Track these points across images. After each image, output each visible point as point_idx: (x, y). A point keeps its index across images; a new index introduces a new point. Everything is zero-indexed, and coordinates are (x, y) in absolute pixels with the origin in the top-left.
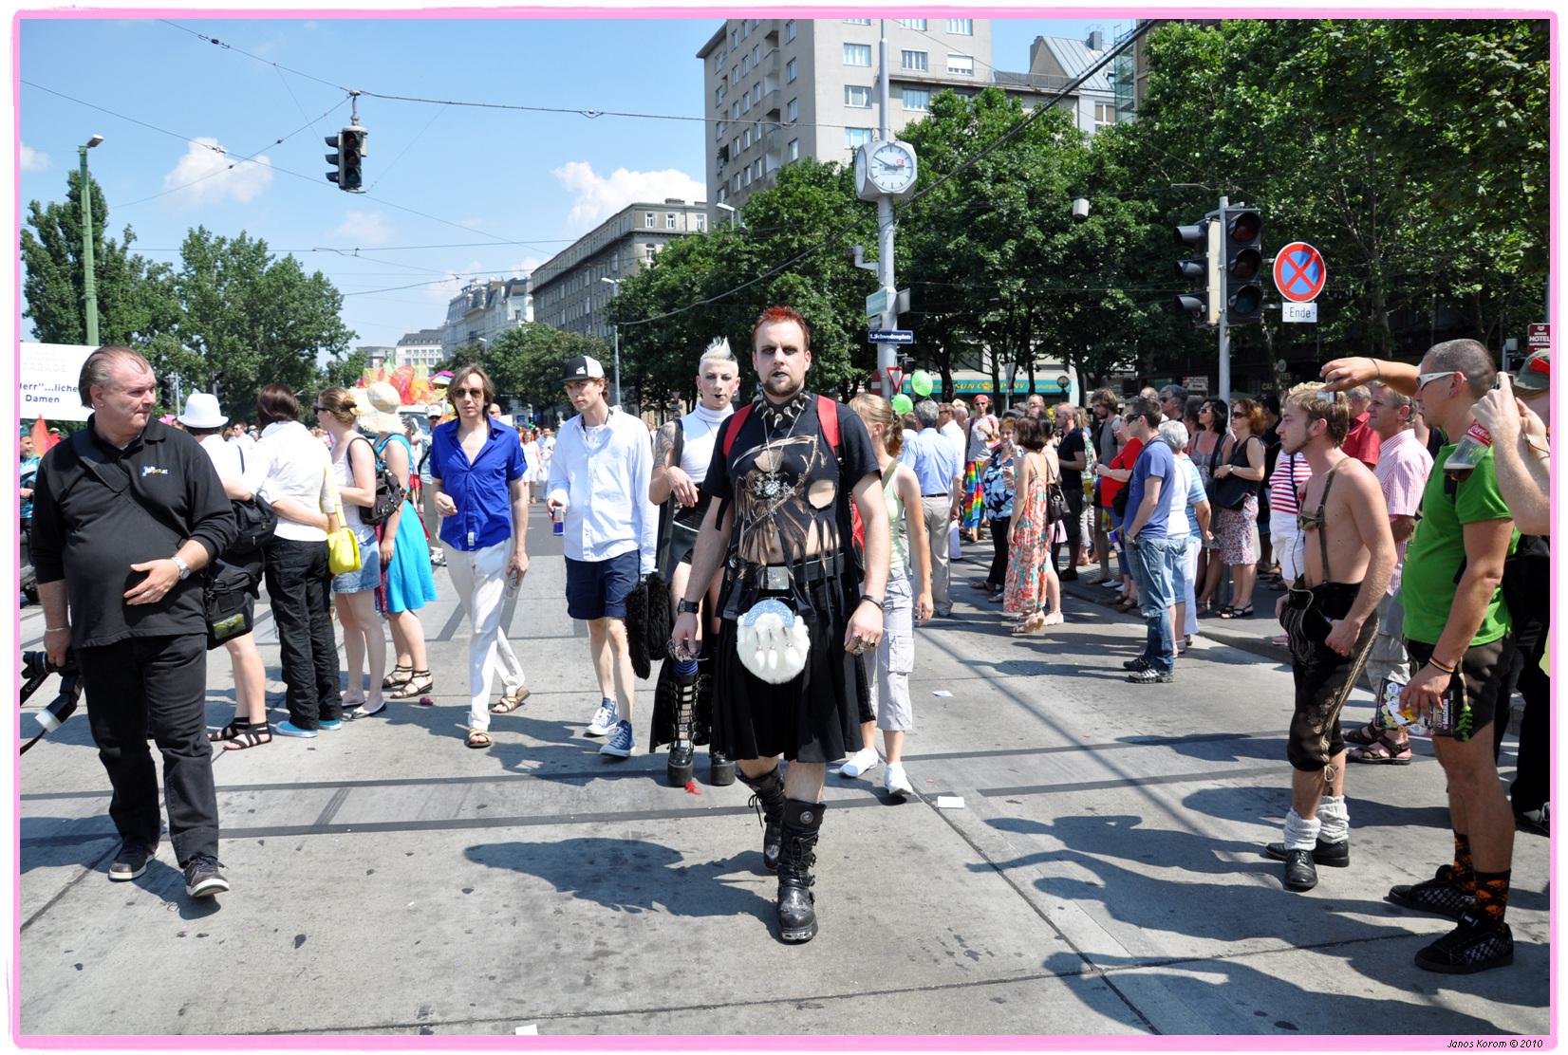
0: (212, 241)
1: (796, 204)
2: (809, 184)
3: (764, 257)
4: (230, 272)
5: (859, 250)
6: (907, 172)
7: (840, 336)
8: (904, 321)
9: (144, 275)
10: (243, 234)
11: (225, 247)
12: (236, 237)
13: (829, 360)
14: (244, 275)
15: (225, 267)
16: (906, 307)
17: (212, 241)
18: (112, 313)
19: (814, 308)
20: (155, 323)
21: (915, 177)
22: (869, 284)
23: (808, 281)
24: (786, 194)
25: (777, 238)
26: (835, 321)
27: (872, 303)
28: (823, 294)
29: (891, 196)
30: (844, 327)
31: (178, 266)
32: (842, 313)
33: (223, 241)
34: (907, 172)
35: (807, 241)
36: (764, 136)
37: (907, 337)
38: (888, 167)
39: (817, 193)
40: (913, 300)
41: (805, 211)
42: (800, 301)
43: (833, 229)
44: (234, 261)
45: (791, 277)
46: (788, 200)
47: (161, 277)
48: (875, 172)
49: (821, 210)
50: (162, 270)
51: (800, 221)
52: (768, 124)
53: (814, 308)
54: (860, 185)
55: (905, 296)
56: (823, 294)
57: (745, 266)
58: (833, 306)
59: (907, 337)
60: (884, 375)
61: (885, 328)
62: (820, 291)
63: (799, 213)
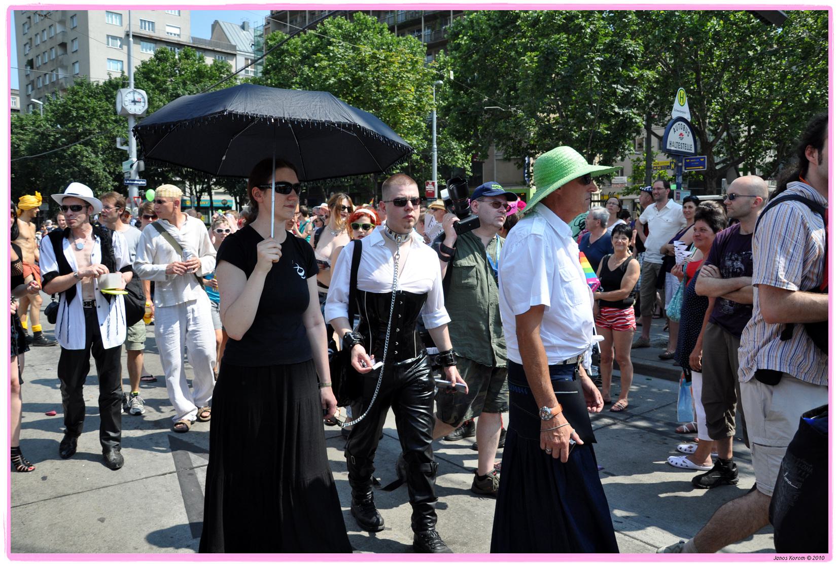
1: (82, 109)
2: (89, 96)
3: (63, 134)
5: (118, 139)
6: (142, 104)
7: (106, 177)
8: (141, 174)
13: (100, 190)
16: (142, 168)
19: (93, 163)
21: (146, 107)
22: (125, 156)
23: (89, 149)
24: (75, 102)
25: (70, 125)
26: (104, 170)
27: (125, 166)
28: (97, 156)
29: (134, 115)
30: (110, 173)
32: (108, 165)
34: (142, 104)
35: (87, 127)
36: (57, 57)
37: (143, 183)
38: (134, 102)
39: (93, 103)
40: (146, 165)
41: (87, 111)
42: (85, 159)
43: (102, 122)
45: (79, 147)
46: (76, 105)
48: (127, 103)
49: (95, 111)
51: (83, 117)
52: (60, 51)
53: (93, 163)
54: (119, 108)
55: (142, 163)
56: (97, 156)
57: (52, 138)
58: (103, 162)
59: (143, 183)
60: (133, 200)
61: (132, 178)
62: (96, 153)
63: (82, 112)
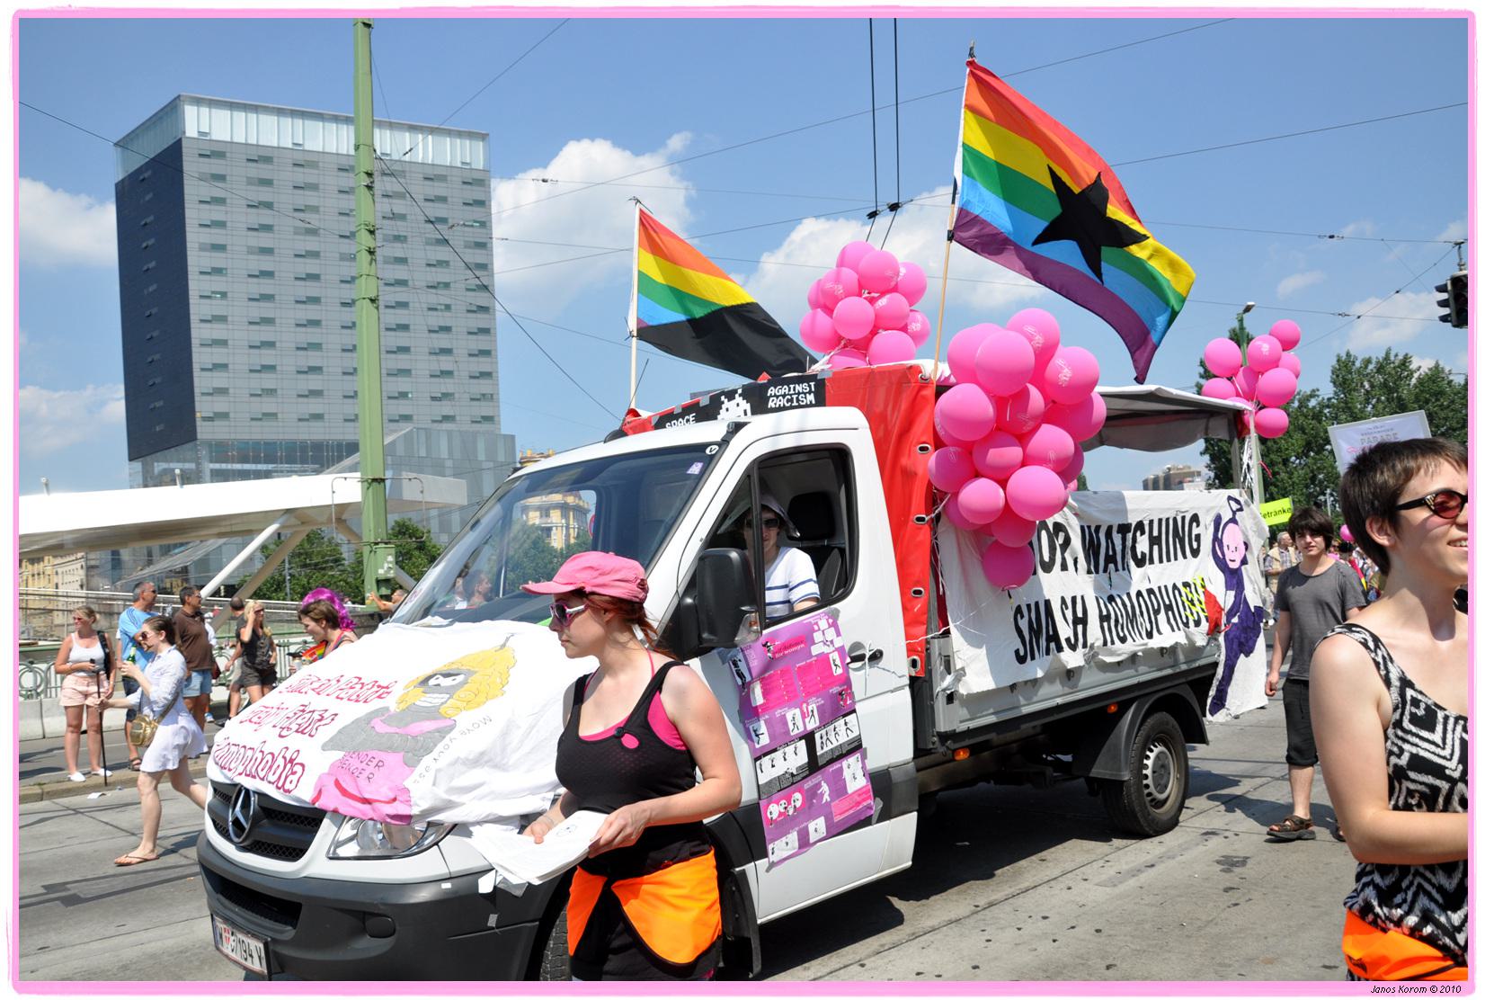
0: (1358, 364)
4: (1377, 392)
9: (1296, 404)
10: (1388, 354)
11: (1371, 367)
12: (1382, 355)
14: (1390, 391)
15: (1372, 386)
17: (1358, 364)
18: (1270, 444)
20: (1308, 446)
31: (1327, 390)
33: (1368, 361)
44: (1380, 378)
47: (1313, 403)
50: (1313, 395)
